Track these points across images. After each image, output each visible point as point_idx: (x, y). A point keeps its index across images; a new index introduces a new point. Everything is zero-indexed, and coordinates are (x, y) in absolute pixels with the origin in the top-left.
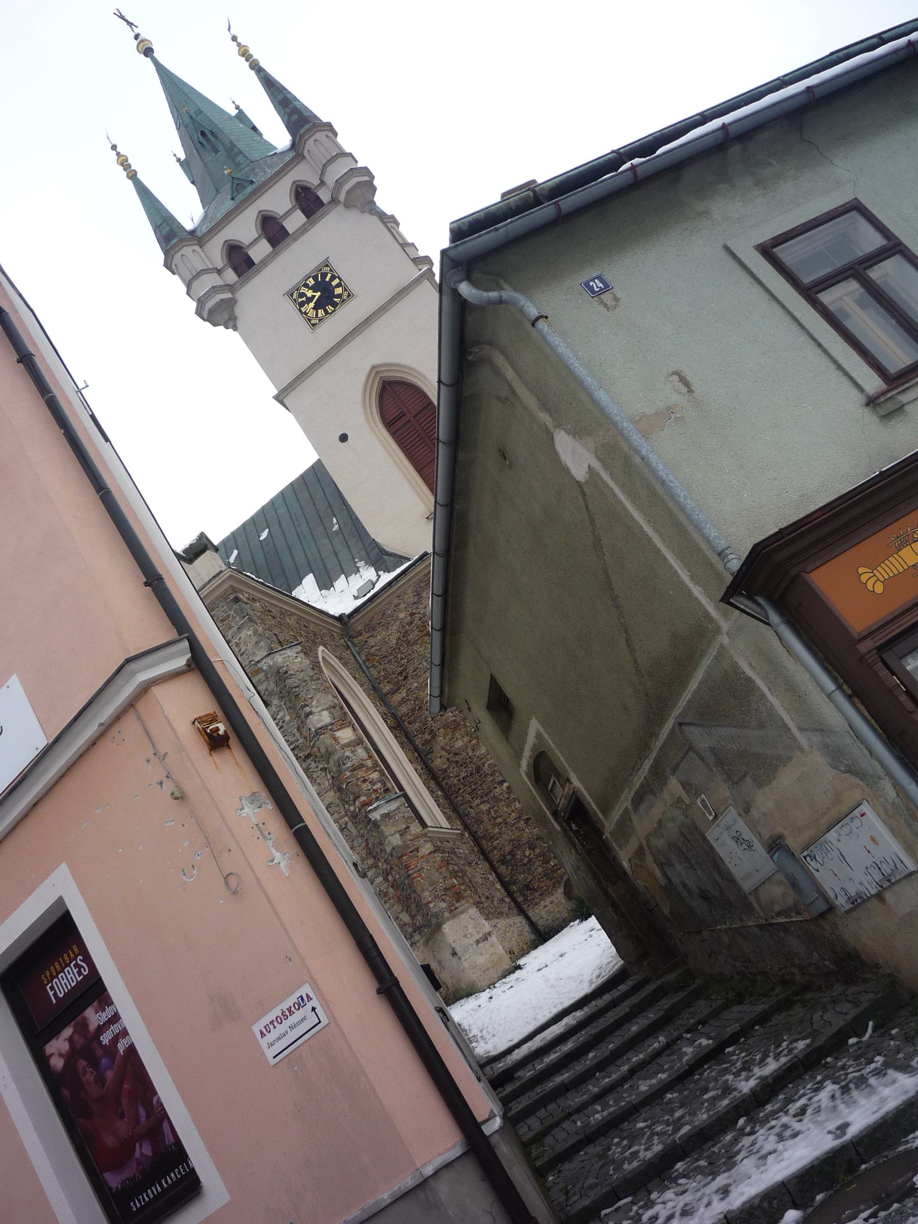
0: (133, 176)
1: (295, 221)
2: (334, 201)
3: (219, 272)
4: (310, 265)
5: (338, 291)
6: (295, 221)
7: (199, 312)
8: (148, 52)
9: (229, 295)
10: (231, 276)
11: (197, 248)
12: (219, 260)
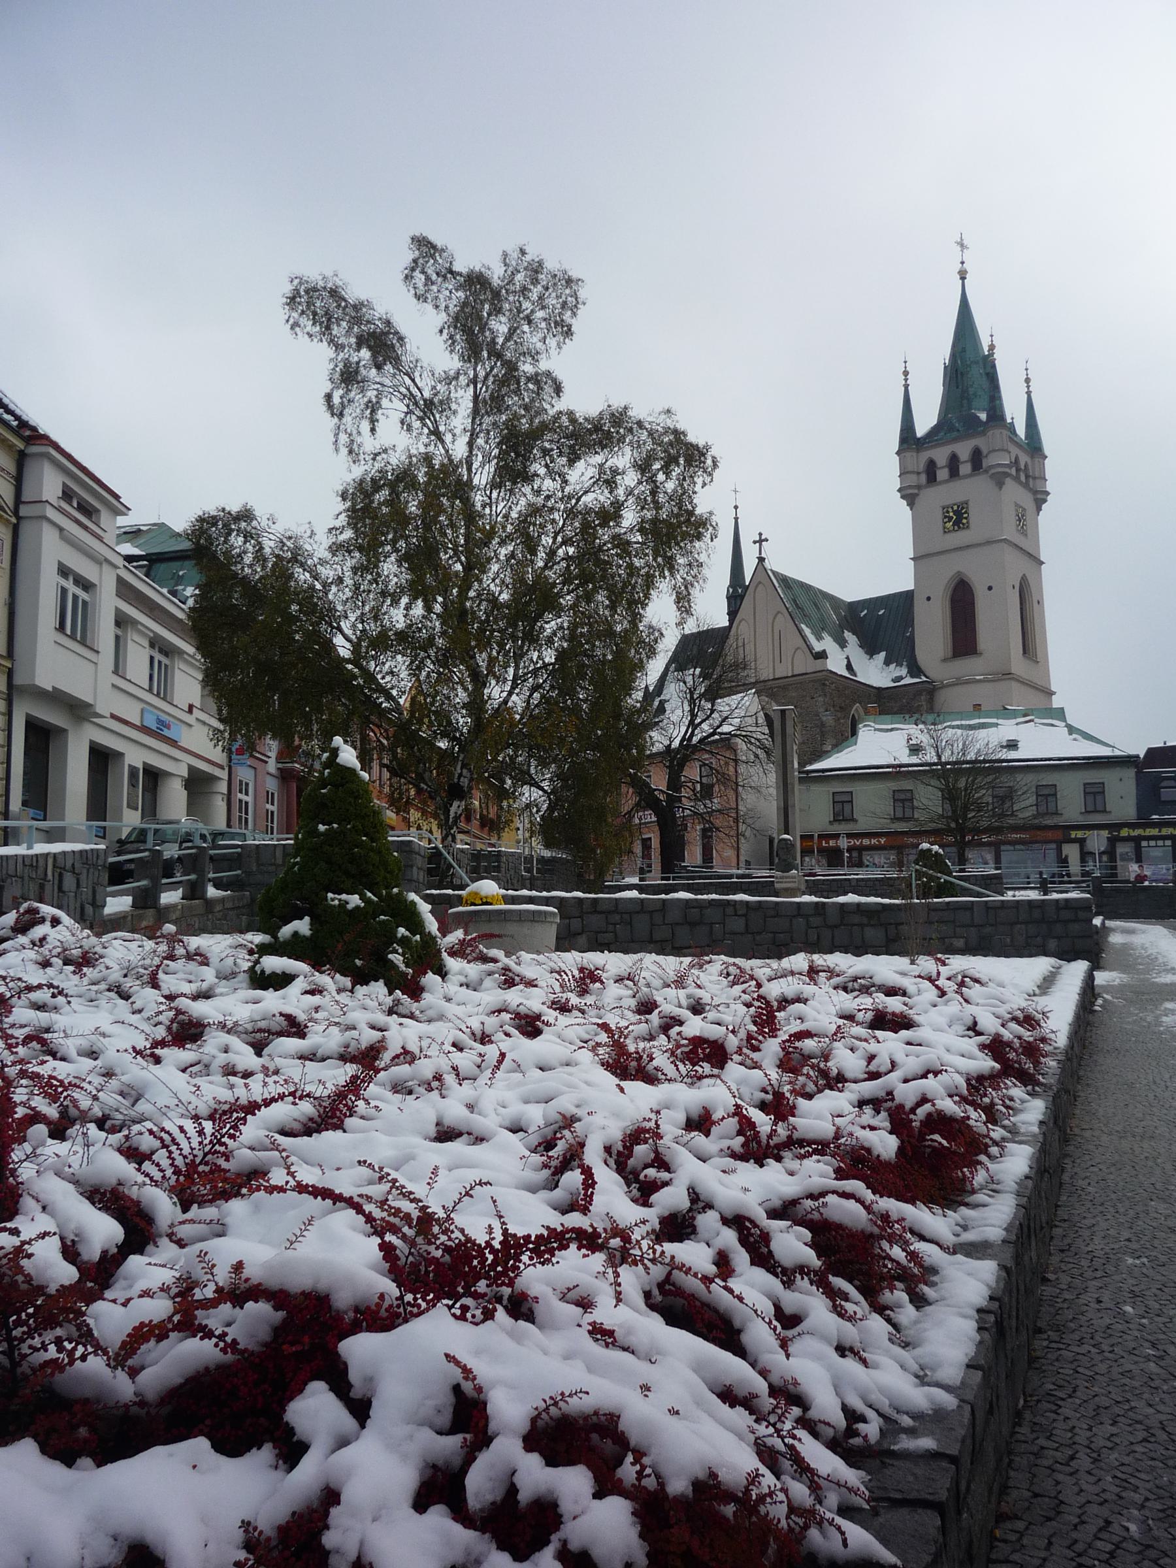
0: (906, 387)
1: (965, 469)
2: (986, 471)
3: (918, 473)
4: (960, 498)
5: (964, 521)
6: (965, 469)
7: (899, 490)
8: (963, 278)
9: (916, 491)
10: (923, 478)
11: (915, 454)
12: (922, 467)
